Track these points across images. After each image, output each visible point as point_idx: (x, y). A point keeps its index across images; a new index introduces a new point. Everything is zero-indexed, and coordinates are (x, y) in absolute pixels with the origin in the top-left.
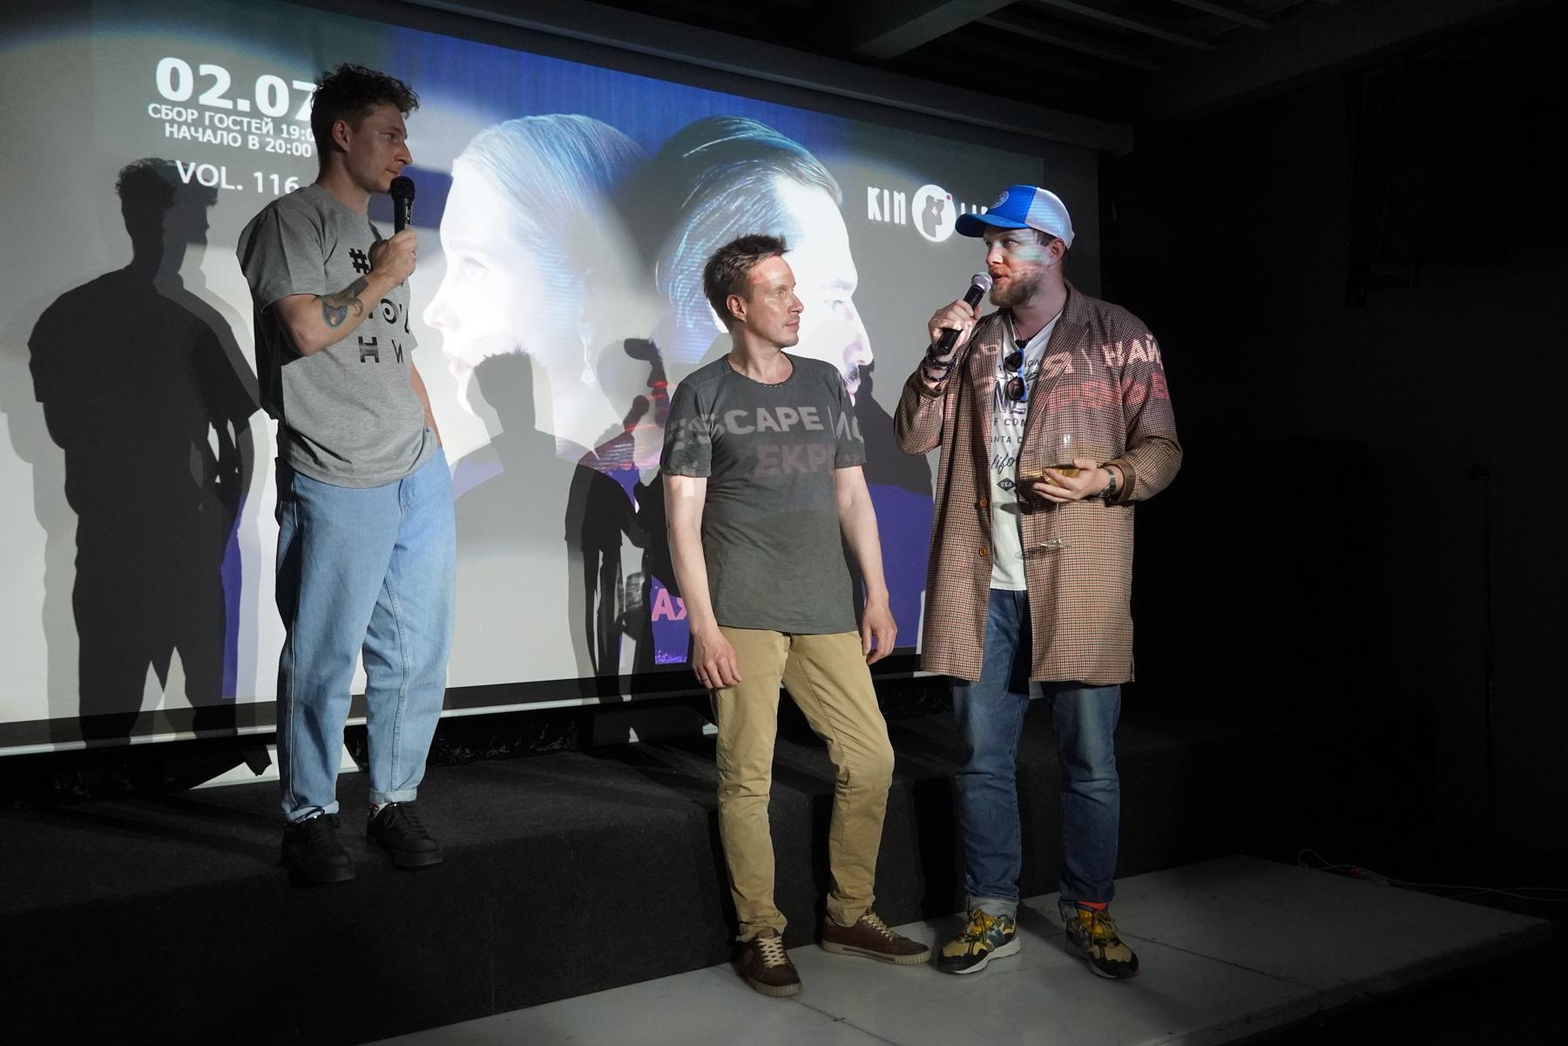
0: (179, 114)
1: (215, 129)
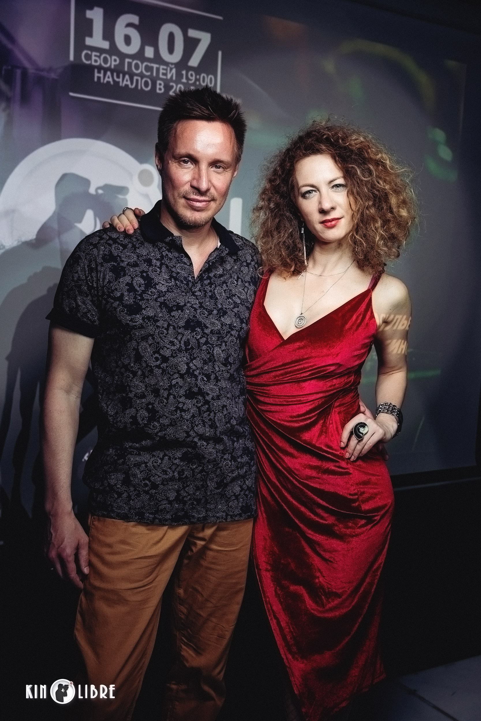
0: (105, 60)
1: (132, 76)
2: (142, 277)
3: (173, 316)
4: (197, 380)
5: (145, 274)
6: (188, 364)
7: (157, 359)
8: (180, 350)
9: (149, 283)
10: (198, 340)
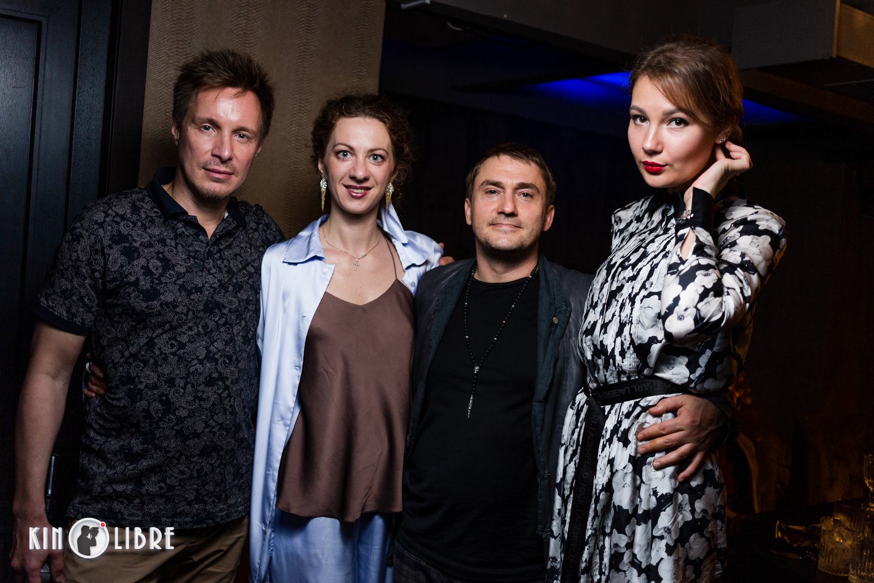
3: (193, 300)
4: (217, 364)
5: (161, 256)
6: (207, 348)
7: (172, 346)
8: (198, 334)
9: (167, 265)
10: (216, 322)
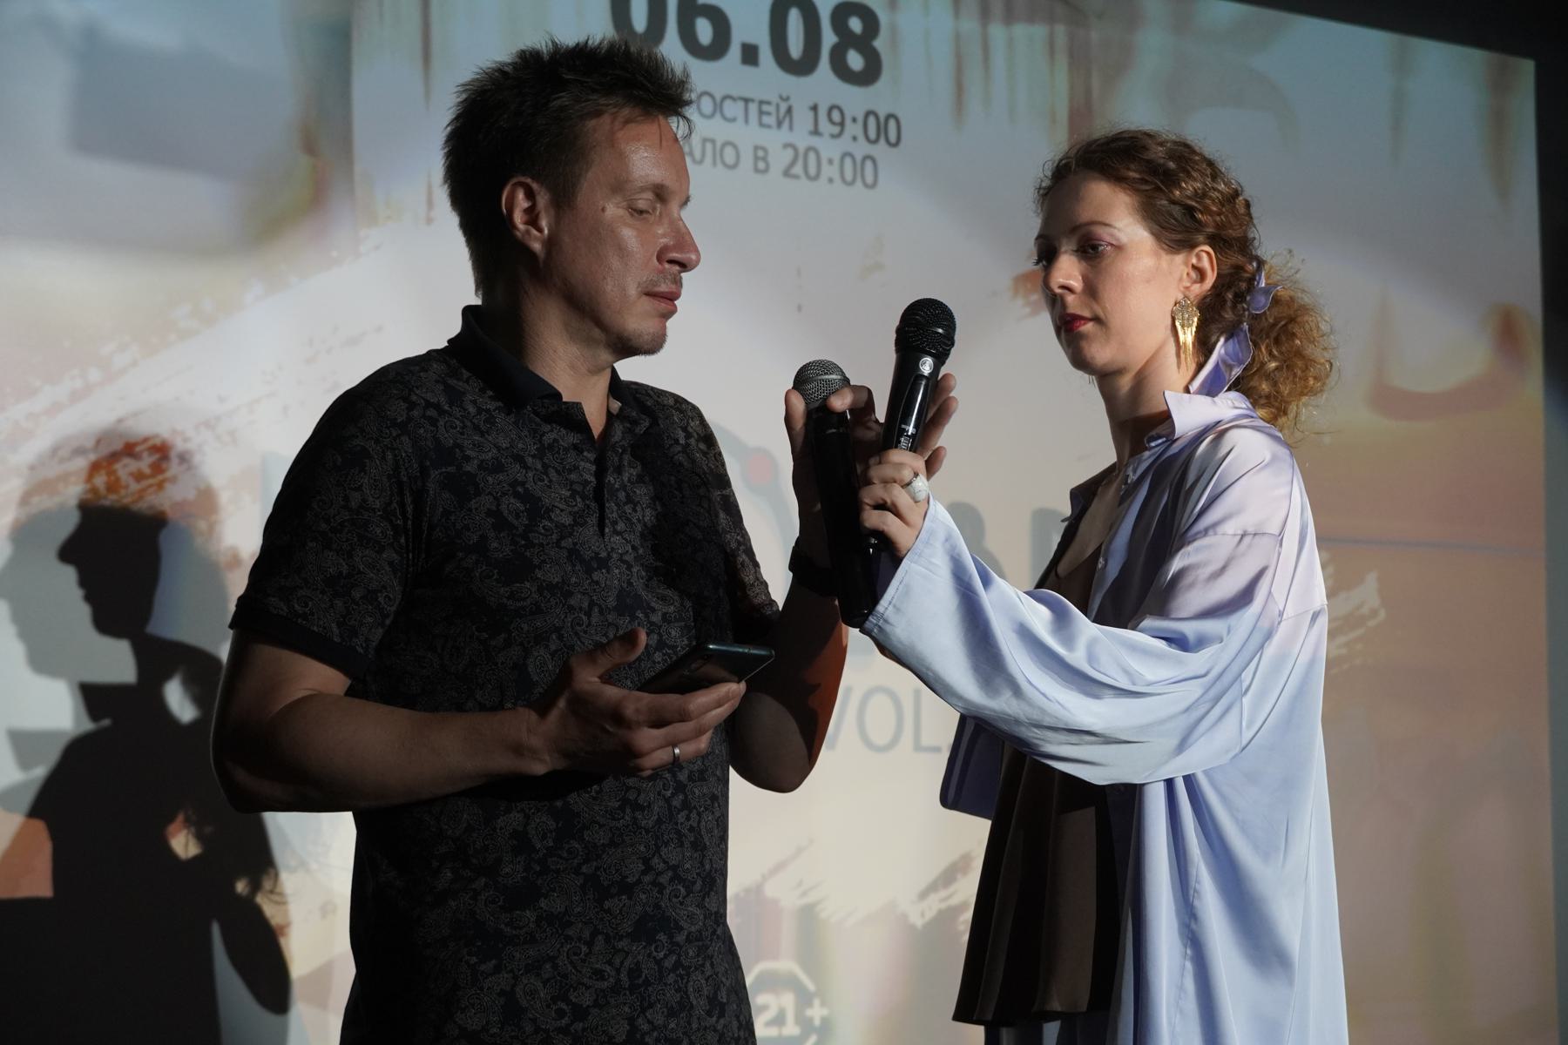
2: (516, 495)
